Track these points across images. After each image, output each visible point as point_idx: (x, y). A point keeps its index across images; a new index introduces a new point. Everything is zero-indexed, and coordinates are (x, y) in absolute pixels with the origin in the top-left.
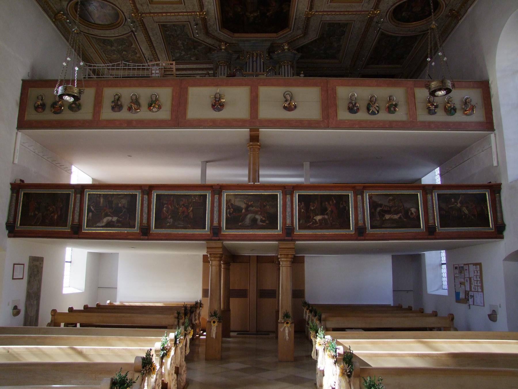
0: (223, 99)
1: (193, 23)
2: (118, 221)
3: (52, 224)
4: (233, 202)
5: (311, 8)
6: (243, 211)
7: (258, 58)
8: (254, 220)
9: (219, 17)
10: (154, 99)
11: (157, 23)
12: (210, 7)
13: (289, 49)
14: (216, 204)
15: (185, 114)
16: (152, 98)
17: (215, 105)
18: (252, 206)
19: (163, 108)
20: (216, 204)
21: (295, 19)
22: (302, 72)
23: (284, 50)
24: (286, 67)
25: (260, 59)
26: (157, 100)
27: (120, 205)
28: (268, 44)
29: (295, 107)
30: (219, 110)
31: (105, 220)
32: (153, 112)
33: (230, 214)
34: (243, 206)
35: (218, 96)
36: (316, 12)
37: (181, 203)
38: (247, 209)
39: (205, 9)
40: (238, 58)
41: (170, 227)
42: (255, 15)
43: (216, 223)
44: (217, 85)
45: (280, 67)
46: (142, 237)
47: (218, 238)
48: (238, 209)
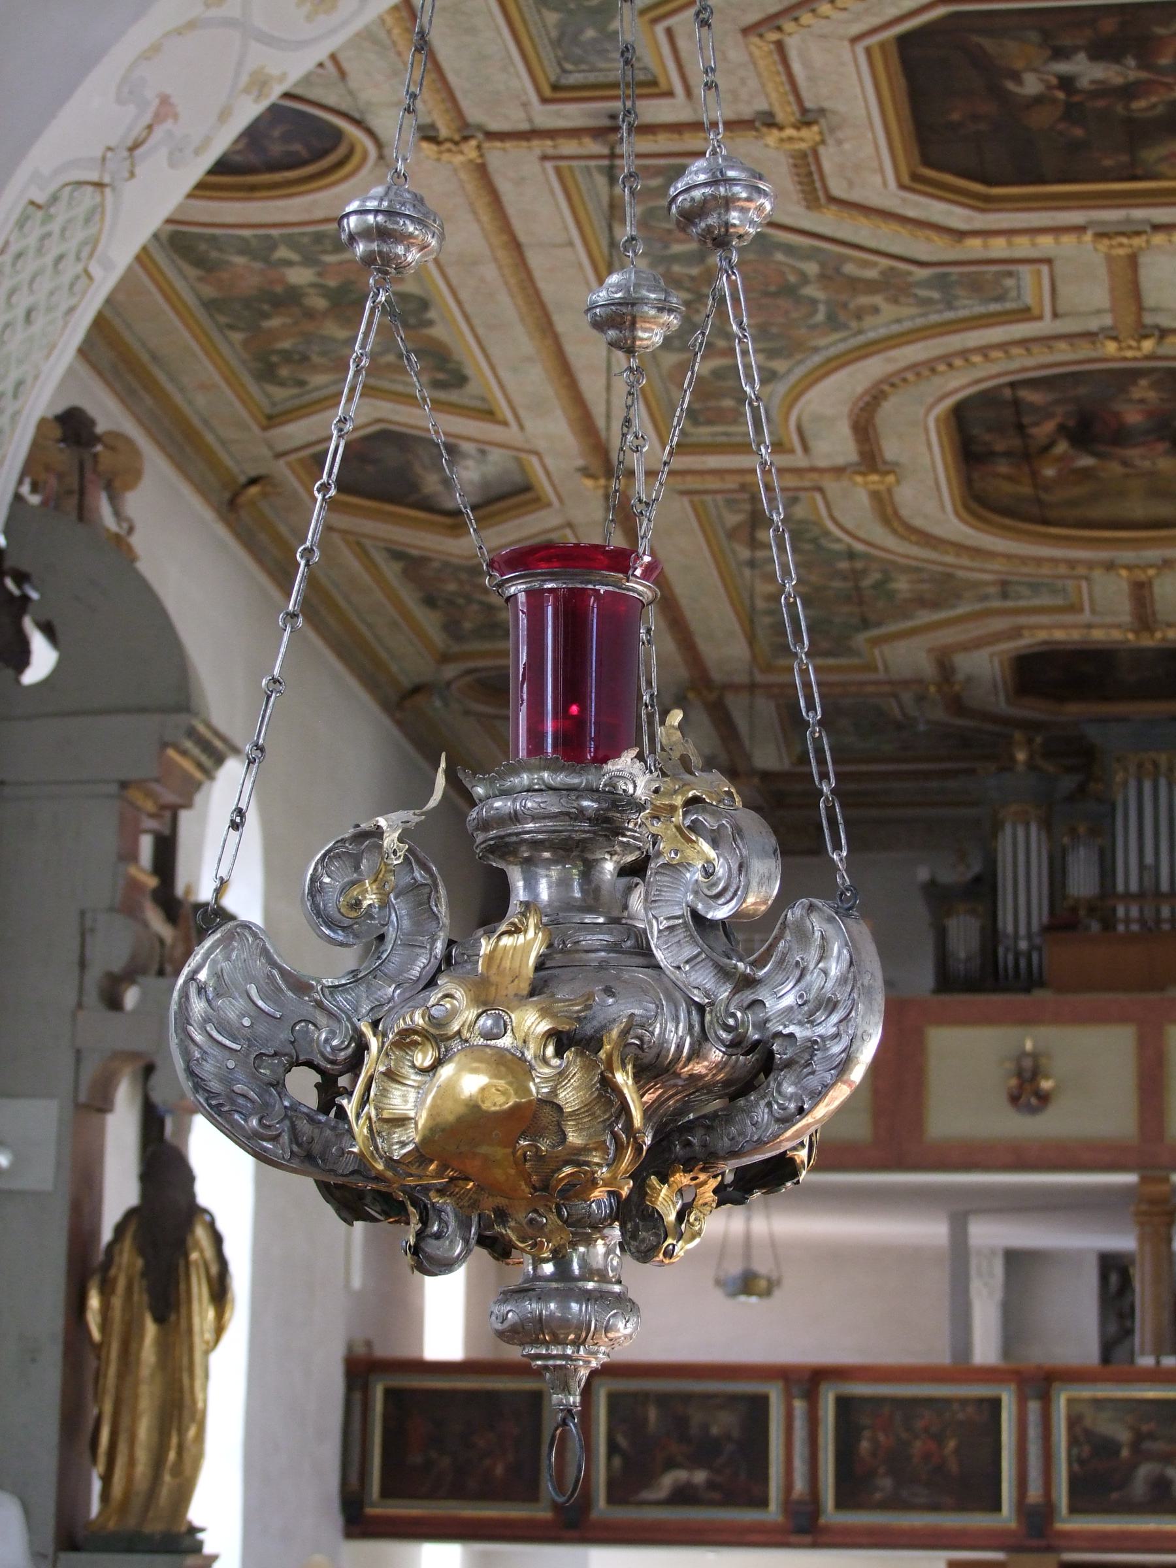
2: (711, 1485)
3: (489, 1493)
4: (1088, 1422)
6: (1125, 1453)
8: (1160, 1485)
14: (1033, 1432)
15: (917, 1121)
18: (1151, 1436)
20: (1033, 1432)
27: (715, 1430)
30: (1033, 1111)
31: (669, 1480)
33: (1082, 1462)
34: (1123, 1435)
37: (919, 1424)
38: (1136, 1445)
40: (1082, 789)
41: (887, 1505)
43: (1034, 1493)
44: (1027, 1020)
46: (793, 1539)
47: (1043, 1543)
48: (1105, 1448)
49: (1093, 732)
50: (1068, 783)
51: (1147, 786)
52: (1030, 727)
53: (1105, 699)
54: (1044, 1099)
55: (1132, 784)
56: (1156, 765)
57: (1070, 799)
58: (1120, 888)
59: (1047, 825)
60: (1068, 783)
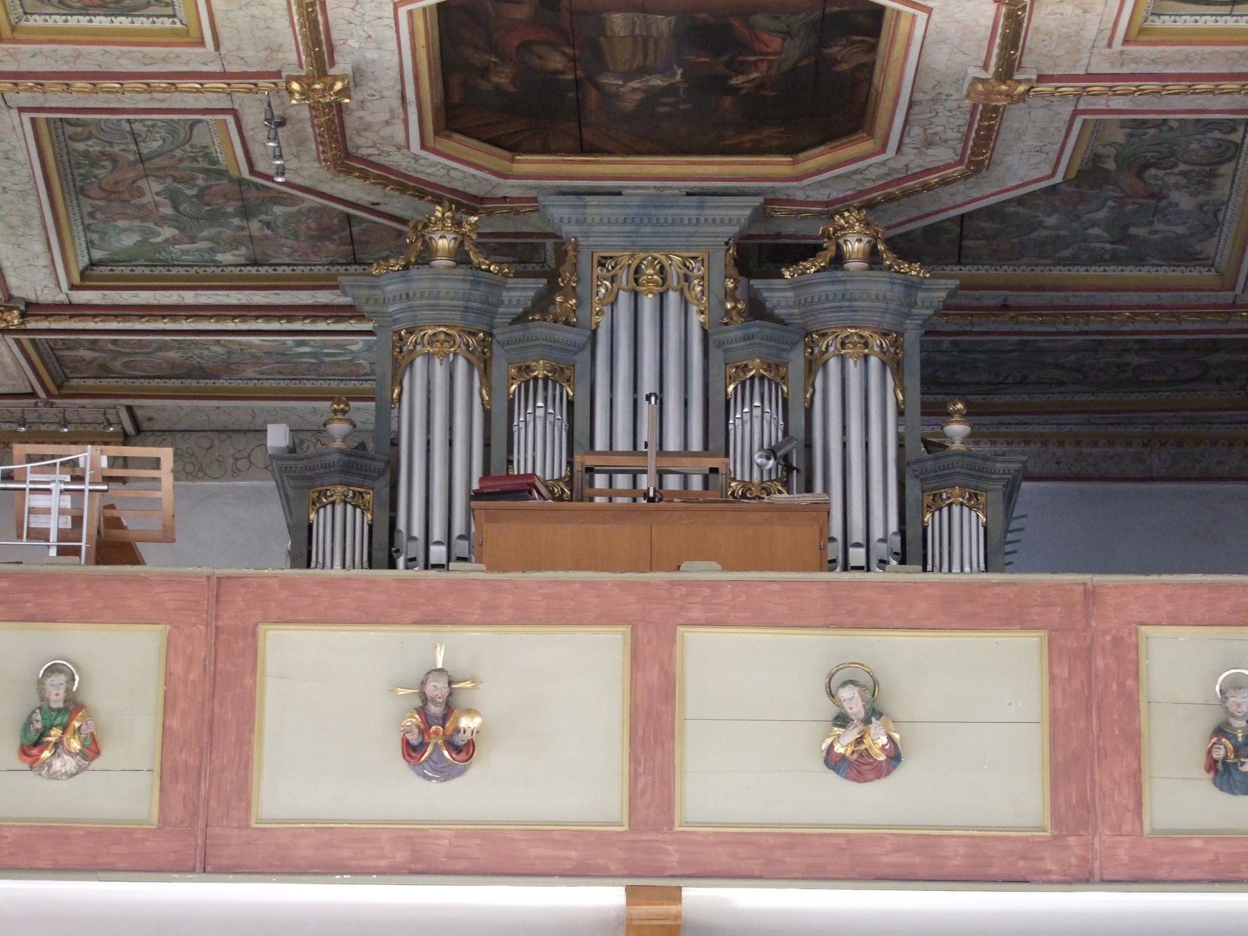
0: (470, 712)
1: (254, 116)
5: (1008, 69)
7: (673, 297)
9: (421, 41)
10: (57, 701)
11: (26, 117)
12: (372, 55)
13: (873, 258)
15: (243, 790)
16: (43, 698)
17: (422, 746)
19: (106, 754)
21: (911, 104)
22: (960, 406)
23: (839, 260)
24: (854, 371)
25: (685, 304)
26: (73, 706)
28: (737, 214)
29: (895, 757)
30: (446, 773)
32: (54, 776)
35: (437, 688)
36: (1042, 78)
39: (343, 66)
40: (542, 304)
42: (657, 81)
45: (814, 365)
49: (560, 213)
50: (521, 292)
51: (648, 303)
52: (466, 203)
53: (585, 149)
54: (464, 750)
55: (624, 299)
56: (662, 270)
57: (521, 319)
58: (600, 444)
59: (483, 363)
60: (521, 292)
